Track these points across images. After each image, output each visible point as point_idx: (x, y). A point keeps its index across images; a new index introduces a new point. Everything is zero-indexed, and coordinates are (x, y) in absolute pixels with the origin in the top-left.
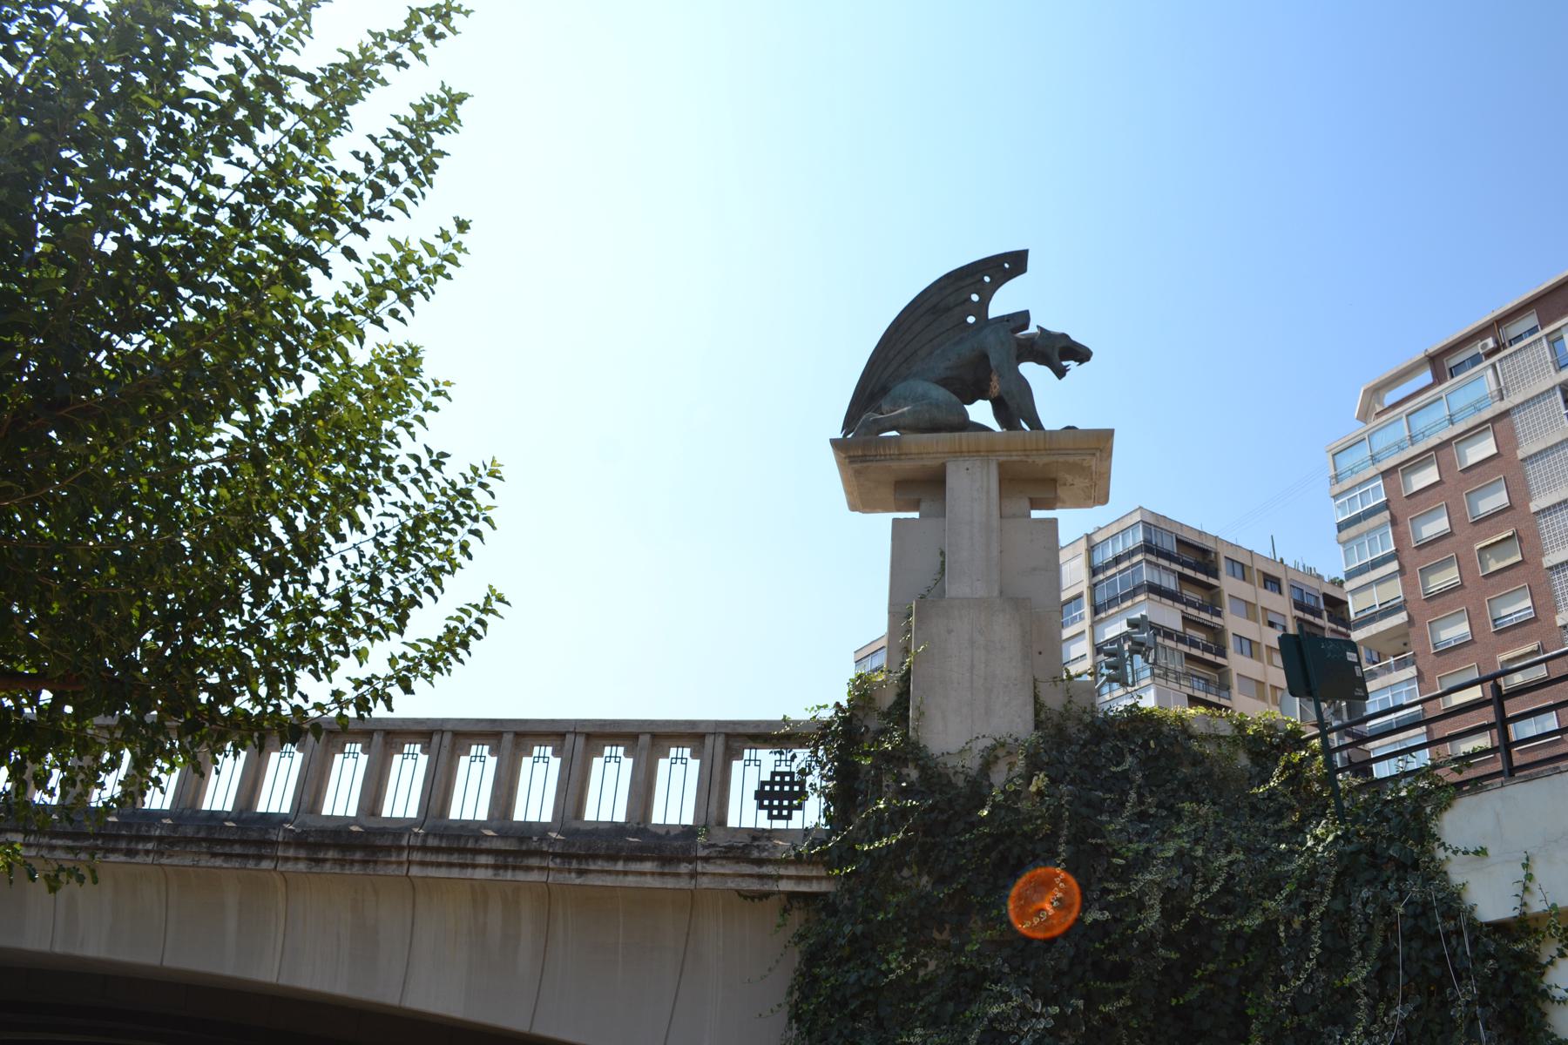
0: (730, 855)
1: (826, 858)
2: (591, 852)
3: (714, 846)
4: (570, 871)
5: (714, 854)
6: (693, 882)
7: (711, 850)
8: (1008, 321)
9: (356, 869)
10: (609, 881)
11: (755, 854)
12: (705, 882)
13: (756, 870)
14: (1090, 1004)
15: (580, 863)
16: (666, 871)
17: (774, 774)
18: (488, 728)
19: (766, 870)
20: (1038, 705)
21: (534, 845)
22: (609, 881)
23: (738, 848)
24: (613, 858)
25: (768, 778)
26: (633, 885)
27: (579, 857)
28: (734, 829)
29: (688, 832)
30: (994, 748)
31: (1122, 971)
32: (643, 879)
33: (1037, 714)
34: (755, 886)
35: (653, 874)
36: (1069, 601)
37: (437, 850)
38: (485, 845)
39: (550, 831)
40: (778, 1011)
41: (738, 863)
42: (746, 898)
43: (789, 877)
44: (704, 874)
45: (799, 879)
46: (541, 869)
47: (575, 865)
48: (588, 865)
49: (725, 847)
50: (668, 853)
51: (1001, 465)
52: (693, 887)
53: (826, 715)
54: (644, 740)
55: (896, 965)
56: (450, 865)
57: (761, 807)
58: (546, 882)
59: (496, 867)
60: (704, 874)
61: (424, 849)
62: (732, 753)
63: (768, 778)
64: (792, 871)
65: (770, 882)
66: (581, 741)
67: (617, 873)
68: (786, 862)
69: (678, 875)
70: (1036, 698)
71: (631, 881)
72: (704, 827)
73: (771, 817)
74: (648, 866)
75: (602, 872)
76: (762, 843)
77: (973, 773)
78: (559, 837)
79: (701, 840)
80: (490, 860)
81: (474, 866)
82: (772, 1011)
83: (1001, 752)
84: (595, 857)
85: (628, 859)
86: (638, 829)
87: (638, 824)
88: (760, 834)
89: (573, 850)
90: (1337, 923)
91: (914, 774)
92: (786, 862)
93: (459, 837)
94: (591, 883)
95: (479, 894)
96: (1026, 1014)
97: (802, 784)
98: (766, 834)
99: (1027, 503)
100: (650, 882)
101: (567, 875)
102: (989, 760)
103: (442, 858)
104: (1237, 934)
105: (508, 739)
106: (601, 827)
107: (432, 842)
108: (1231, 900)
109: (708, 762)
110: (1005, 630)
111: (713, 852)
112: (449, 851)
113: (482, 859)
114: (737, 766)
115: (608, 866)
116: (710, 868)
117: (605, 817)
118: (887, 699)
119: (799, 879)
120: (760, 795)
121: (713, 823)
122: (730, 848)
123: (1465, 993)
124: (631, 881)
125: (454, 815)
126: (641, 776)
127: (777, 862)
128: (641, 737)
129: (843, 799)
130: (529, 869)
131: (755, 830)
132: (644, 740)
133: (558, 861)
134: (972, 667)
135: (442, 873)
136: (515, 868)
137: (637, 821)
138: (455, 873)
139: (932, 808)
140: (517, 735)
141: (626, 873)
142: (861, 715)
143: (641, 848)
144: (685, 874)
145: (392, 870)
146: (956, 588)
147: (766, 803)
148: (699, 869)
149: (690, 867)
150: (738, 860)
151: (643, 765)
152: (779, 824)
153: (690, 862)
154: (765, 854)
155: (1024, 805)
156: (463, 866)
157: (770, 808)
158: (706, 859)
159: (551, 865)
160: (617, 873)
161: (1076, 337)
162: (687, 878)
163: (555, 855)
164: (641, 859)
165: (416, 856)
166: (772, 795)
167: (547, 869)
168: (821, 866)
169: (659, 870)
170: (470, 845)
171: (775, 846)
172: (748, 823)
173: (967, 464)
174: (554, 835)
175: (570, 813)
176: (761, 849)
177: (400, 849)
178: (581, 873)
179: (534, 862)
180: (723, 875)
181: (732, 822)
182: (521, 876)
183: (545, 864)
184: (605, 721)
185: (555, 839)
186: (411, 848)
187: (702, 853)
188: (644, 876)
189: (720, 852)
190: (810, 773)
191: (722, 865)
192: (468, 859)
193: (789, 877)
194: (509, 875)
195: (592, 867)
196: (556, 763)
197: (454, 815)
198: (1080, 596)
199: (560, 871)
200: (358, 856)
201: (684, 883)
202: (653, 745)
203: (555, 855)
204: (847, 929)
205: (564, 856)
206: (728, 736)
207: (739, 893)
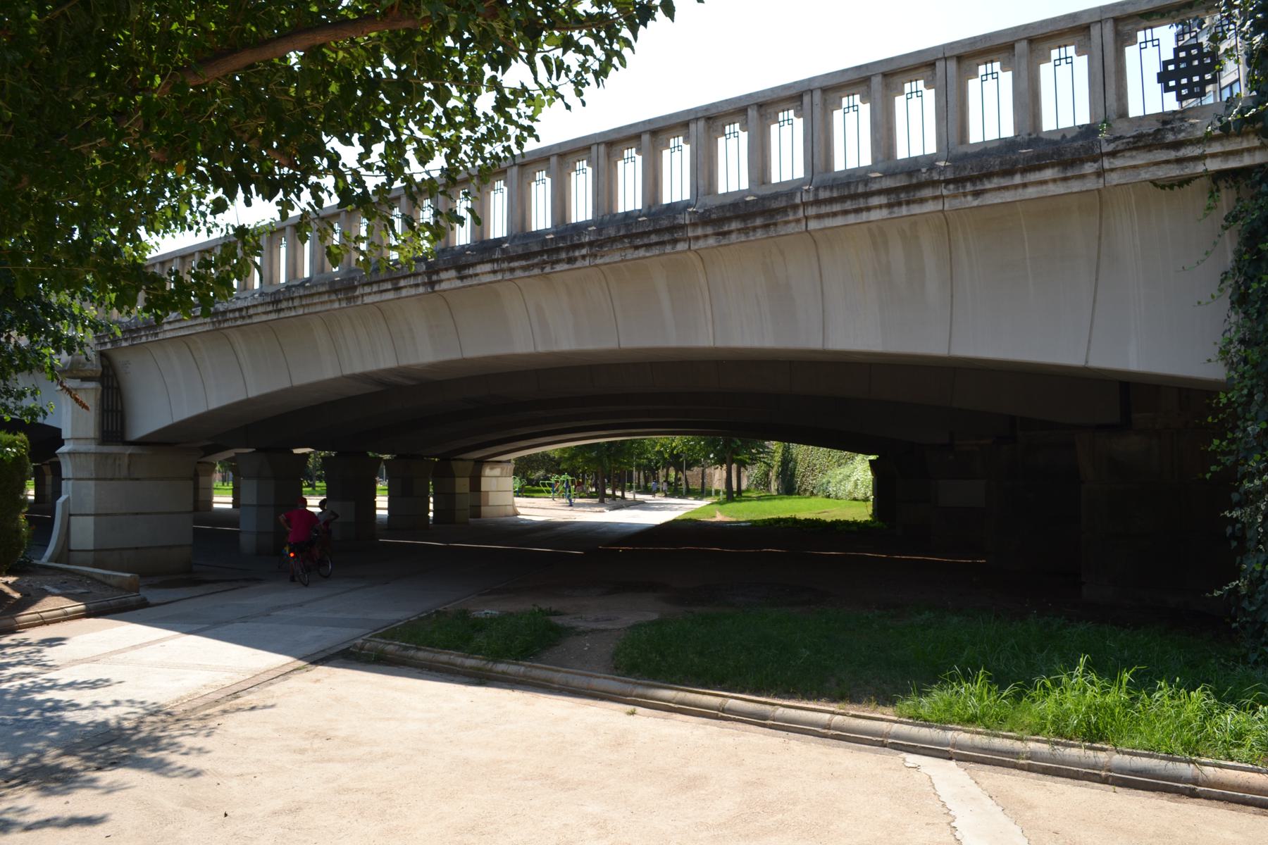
0: (1141, 144)
1: (1259, 125)
2: (984, 171)
3: (1120, 138)
4: (965, 195)
5: (1121, 147)
6: (1101, 181)
7: (1117, 143)
9: (760, 234)
10: (1008, 196)
11: (1170, 137)
12: (1114, 179)
13: (1172, 155)
15: (974, 184)
16: (1069, 174)
17: (1177, 51)
18: (855, 76)
19: (1183, 152)
21: (924, 176)
22: (1008, 196)
23: (1149, 135)
24: (1009, 173)
25: (1171, 56)
26: (1034, 196)
27: (972, 179)
28: (1139, 118)
29: (1087, 132)
32: (1044, 187)
34: (1174, 172)
35: (1054, 181)
37: (831, 201)
38: (875, 187)
39: (936, 161)
40: (1219, 296)
41: (1150, 151)
42: (1163, 187)
43: (1214, 156)
44: (1112, 170)
45: (1226, 155)
46: (935, 198)
47: (969, 187)
48: (983, 184)
49: (1134, 137)
50: (1069, 156)
52: (1101, 185)
54: (1021, 47)
56: (845, 212)
57: (1167, 89)
58: (943, 211)
59: (890, 206)
60: (1112, 170)
61: (817, 202)
62: (1124, 39)
63: (1171, 56)
64: (1216, 148)
65: (1192, 164)
66: (952, 65)
67: (1016, 187)
68: (1208, 139)
69: (1083, 177)
71: (1031, 192)
72: (1105, 122)
73: (1180, 98)
74: (1048, 174)
75: (999, 189)
76: (1177, 124)
78: (947, 164)
80: (883, 200)
81: (868, 209)
82: (1213, 297)
84: (989, 175)
85: (1024, 171)
86: (1030, 140)
87: (1030, 135)
88: (1171, 117)
89: (965, 173)
92: (1208, 139)
93: (848, 184)
94: (990, 202)
97: (1213, 54)
98: (1179, 116)
100: (1053, 189)
101: (963, 199)
103: (837, 207)
105: (877, 82)
106: (989, 146)
107: (823, 195)
109: (1098, 53)
111: (1120, 145)
112: (842, 199)
113: (875, 201)
114: (1131, 52)
116: (1118, 162)
117: (992, 135)
119: (1226, 155)
120: (1163, 77)
121: (1113, 116)
122: (1140, 137)
124: (1031, 192)
125: (839, 166)
126: (1024, 84)
127: (1199, 141)
128: (1017, 46)
130: (922, 201)
131: (1164, 114)
132: (1021, 47)
133: (951, 187)
135: (839, 221)
136: (908, 203)
137: (1028, 131)
138: (851, 219)
140: (885, 75)
141: (1025, 185)
143: (1038, 157)
144: (1090, 174)
145: (792, 228)
147: (1172, 83)
148: (1107, 165)
149: (1096, 165)
150: (1149, 148)
151: (1024, 74)
152: (1192, 102)
153: (1095, 161)
154: (1181, 136)
156: (858, 211)
157: (1178, 89)
158: (1113, 154)
159: (945, 192)
160: (1016, 187)
162: (1094, 177)
163: (947, 182)
164: (1040, 168)
165: (812, 211)
166: (1176, 75)
167: (942, 197)
168: (1252, 136)
169: (1061, 175)
170: (861, 189)
171: (1193, 125)
172: (1154, 108)
174: (942, 164)
175: (954, 139)
177: (795, 207)
178: (977, 194)
179: (927, 192)
180: (1135, 167)
181: (1135, 110)
182: (916, 209)
183: (938, 193)
184: (975, 37)
186: (805, 205)
187: (1107, 148)
189: (1128, 143)
190: (1224, 38)
191: (1132, 157)
192: (861, 203)
193: (1214, 156)
194: (904, 211)
195: (988, 186)
196: (930, 95)
197: (839, 166)
199: (955, 196)
200: (759, 222)
201: (1091, 184)
202: (1031, 51)
203: (947, 182)
205: (958, 181)
206: (1116, 20)
207: (1153, 182)
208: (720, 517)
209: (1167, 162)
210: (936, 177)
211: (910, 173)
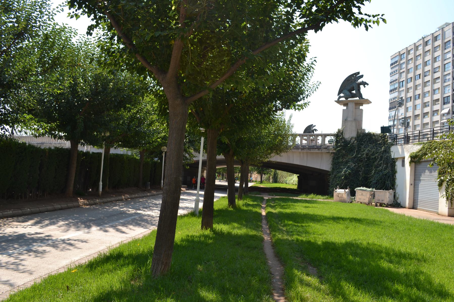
12: (323, 151)
14: (358, 164)
20: (358, 132)
31: (362, 161)
33: (358, 133)
34: (328, 152)
36: (447, 42)
53: (335, 133)
55: (341, 160)
71: (315, 151)
90: (382, 157)
91: (343, 140)
95: (300, 152)
96: (352, 165)
100: (317, 151)
102: (351, 139)
104: (372, 158)
108: (373, 154)
110: (354, 124)
118: (341, 132)
123: (389, 164)
124: (315, 151)
129: (337, 142)
146: (349, 119)
155: (354, 144)
161: (367, 82)
188: (316, 151)
198: (450, 41)
201: (321, 151)
205: (308, 149)
208: (262, 186)
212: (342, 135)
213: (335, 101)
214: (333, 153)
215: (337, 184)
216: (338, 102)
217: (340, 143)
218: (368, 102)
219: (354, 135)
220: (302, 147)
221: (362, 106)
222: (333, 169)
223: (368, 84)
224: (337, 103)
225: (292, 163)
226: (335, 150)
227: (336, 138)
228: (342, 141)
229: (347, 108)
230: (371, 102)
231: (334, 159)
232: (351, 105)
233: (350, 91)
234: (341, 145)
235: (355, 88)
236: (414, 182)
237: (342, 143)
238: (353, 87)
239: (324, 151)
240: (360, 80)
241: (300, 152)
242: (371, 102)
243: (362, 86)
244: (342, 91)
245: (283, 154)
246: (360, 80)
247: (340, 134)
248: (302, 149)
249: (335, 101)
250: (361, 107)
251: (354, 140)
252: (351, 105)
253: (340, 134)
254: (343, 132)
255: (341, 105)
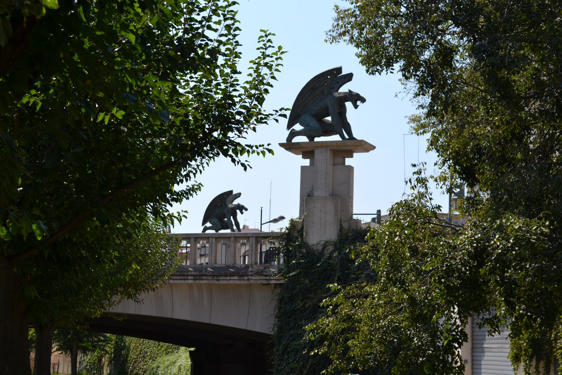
3: (253, 271)
4: (215, 280)
8: (345, 78)
10: (226, 282)
11: (264, 274)
12: (252, 282)
13: (265, 278)
18: (186, 236)
19: (268, 278)
20: (341, 229)
22: (226, 282)
24: (226, 276)
27: (217, 276)
30: (325, 244)
34: (265, 282)
35: (237, 280)
38: (190, 274)
43: (274, 280)
46: (206, 279)
47: (216, 278)
51: (330, 150)
53: (283, 231)
55: (299, 304)
56: (181, 279)
59: (194, 279)
66: (214, 240)
67: (228, 280)
69: (244, 280)
70: (341, 225)
71: (232, 282)
74: (236, 278)
76: (268, 270)
77: (320, 251)
79: (250, 269)
80: (192, 278)
81: (188, 279)
83: (328, 244)
84: (221, 276)
85: (230, 276)
89: (215, 274)
91: (304, 251)
99: (341, 159)
102: (325, 246)
103: (178, 278)
110: (330, 206)
112: (180, 275)
113: (190, 277)
115: (225, 278)
116: (253, 278)
118: (299, 227)
121: (253, 263)
122: (258, 272)
124: (232, 282)
128: (231, 238)
130: (203, 280)
134: (321, 218)
135: (179, 282)
136: (199, 279)
138: (183, 282)
139: (308, 262)
140: (195, 238)
141: (230, 280)
142: (292, 231)
143: (233, 273)
146: (317, 193)
150: (260, 275)
154: (267, 274)
156: (185, 279)
158: (251, 275)
160: (228, 280)
161: (362, 95)
163: (210, 276)
164: (234, 276)
167: (208, 279)
170: (186, 274)
173: (321, 150)
176: (266, 272)
178: (218, 280)
179: (204, 277)
182: (201, 282)
185: (210, 271)
187: (250, 274)
188: (235, 280)
192: (186, 277)
193: (274, 280)
194: (198, 281)
195: (221, 279)
199: (212, 280)
201: (246, 282)
202: (235, 240)
203: (210, 276)
204: (286, 295)
205: (213, 276)
206: (256, 237)
207: (262, 284)
209: (264, 279)
210: (207, 274)
211: (200, 272)
212: (302, 235)
213: (281, 145)
214: (280, 284)
215: (292, 369)
216: (289, 146)
217: (295, 257)
218: (366, 147)
219: (331, 234)
220: (195, 271)
221: (351, 156)
222: (280, 329)
223: (363, 100)
224: (287, 149)
225: (169, 316)
226: (285, 278)
227: (286, 245)
228: (300, 252)
229: (311, 163)
230: (373, 148)
231: (281, 301)
232: (321, 156)
233: (319, 118)
234: (298, 264)
235: (330, 112)
236: (473, 356)
237: (302, 258)
238: (327, 109)
239: (256, 280)
240: (344, 89)
241: (190, 286)
242: (373, 148)
243: (349, 105)
244: (299, 116)
245: (142, 296)
246: (344, 89)
247: (296, 234)
248: (196, 277)
249: (281, 145)
250: (348, 161)
251: (331, 248)
252: (321, 156)
253: (296, 234)
254: (302, 228)
255: (297, 154)
